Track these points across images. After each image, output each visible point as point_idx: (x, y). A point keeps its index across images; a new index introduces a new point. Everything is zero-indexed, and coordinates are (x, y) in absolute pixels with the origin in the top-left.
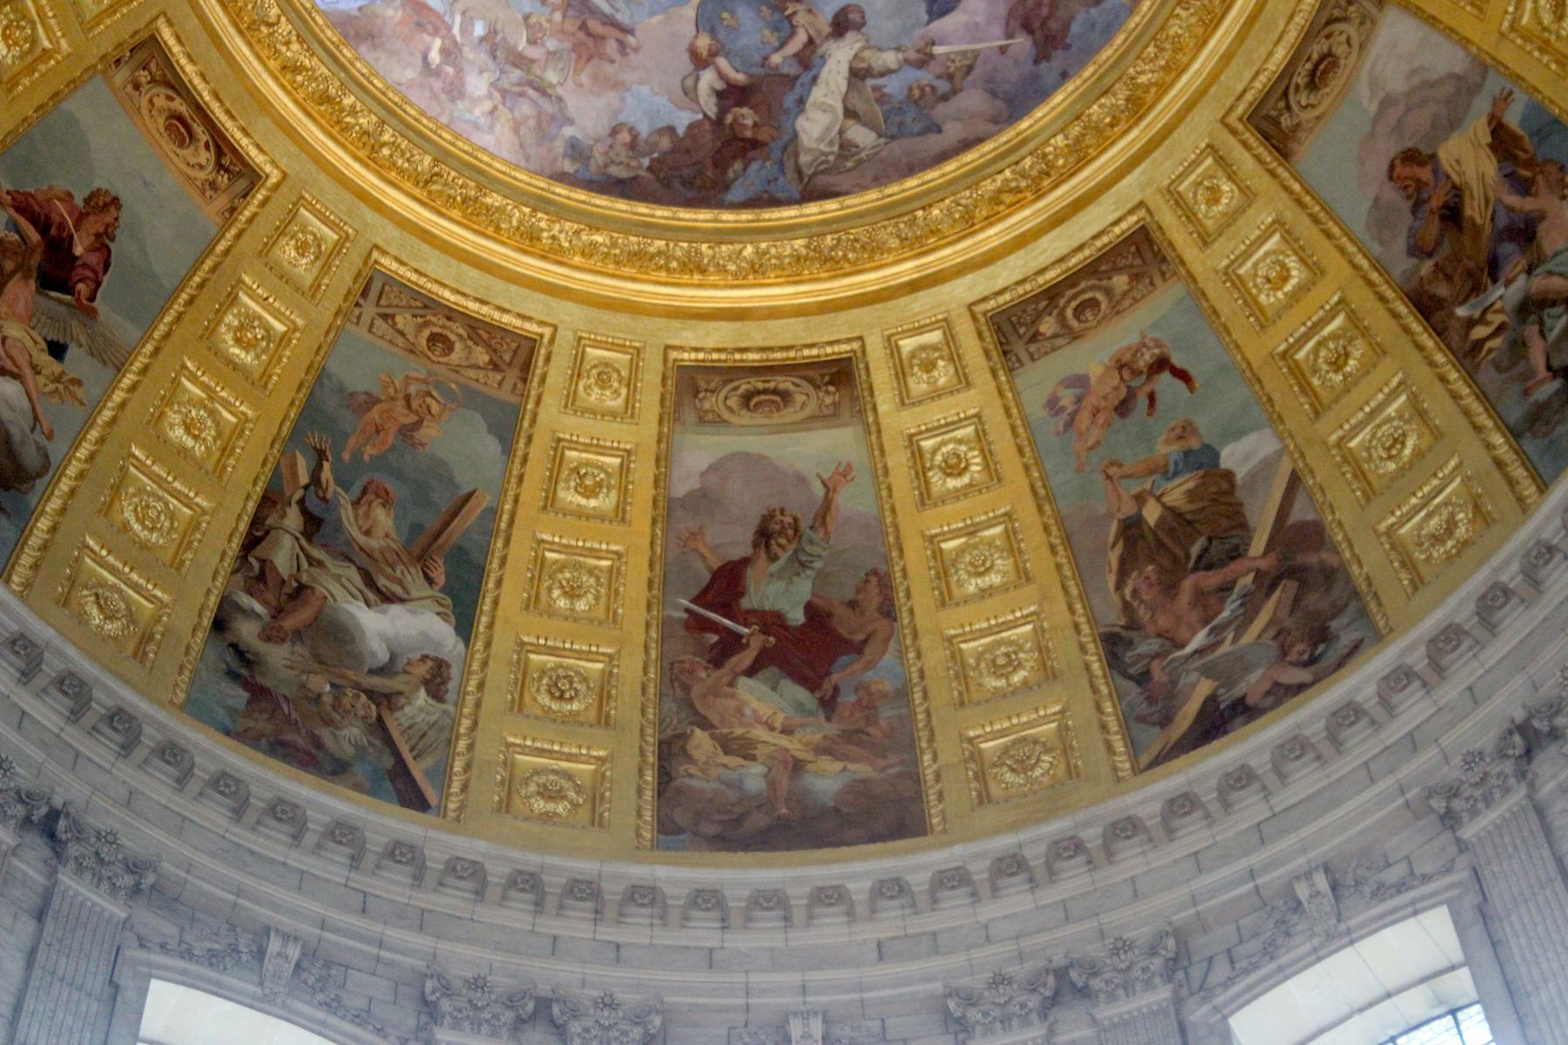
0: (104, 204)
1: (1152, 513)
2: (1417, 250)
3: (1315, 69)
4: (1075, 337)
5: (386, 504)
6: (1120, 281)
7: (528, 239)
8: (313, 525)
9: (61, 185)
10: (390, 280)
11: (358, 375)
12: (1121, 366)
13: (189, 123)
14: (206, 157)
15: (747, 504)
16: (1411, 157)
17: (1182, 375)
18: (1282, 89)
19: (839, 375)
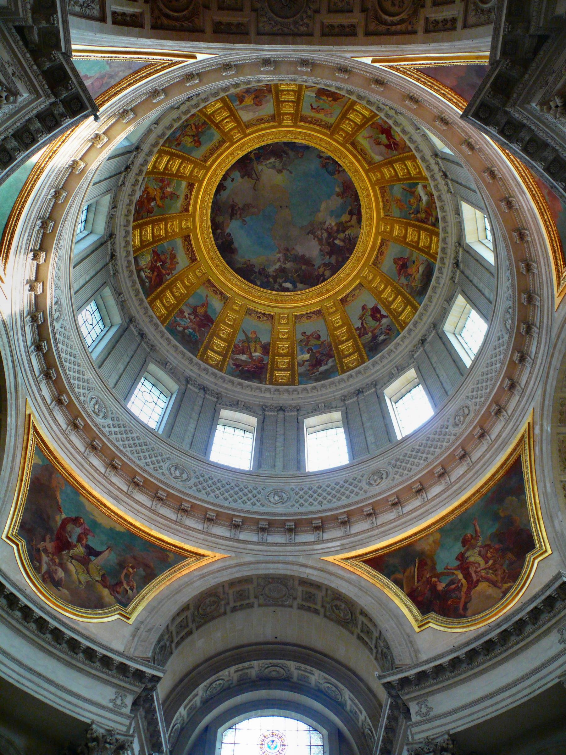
0: (395, 261)
1: (330, 99)
2: (265, 96)
3: (261, 120)
4: (321, 120)
5: (410, 201)
6: (309, 119)
7: (368, 195)
8: (418, 212)
9: (395, 269)
10: (384, 212)
11: (398, 211)
12: (318, 112)
13: (381, 253)
14: (383, 248)
15: (377, 148)
16: (257, 105)
17: (311, 105)
18: (267, 122)
19: (353, 144)
